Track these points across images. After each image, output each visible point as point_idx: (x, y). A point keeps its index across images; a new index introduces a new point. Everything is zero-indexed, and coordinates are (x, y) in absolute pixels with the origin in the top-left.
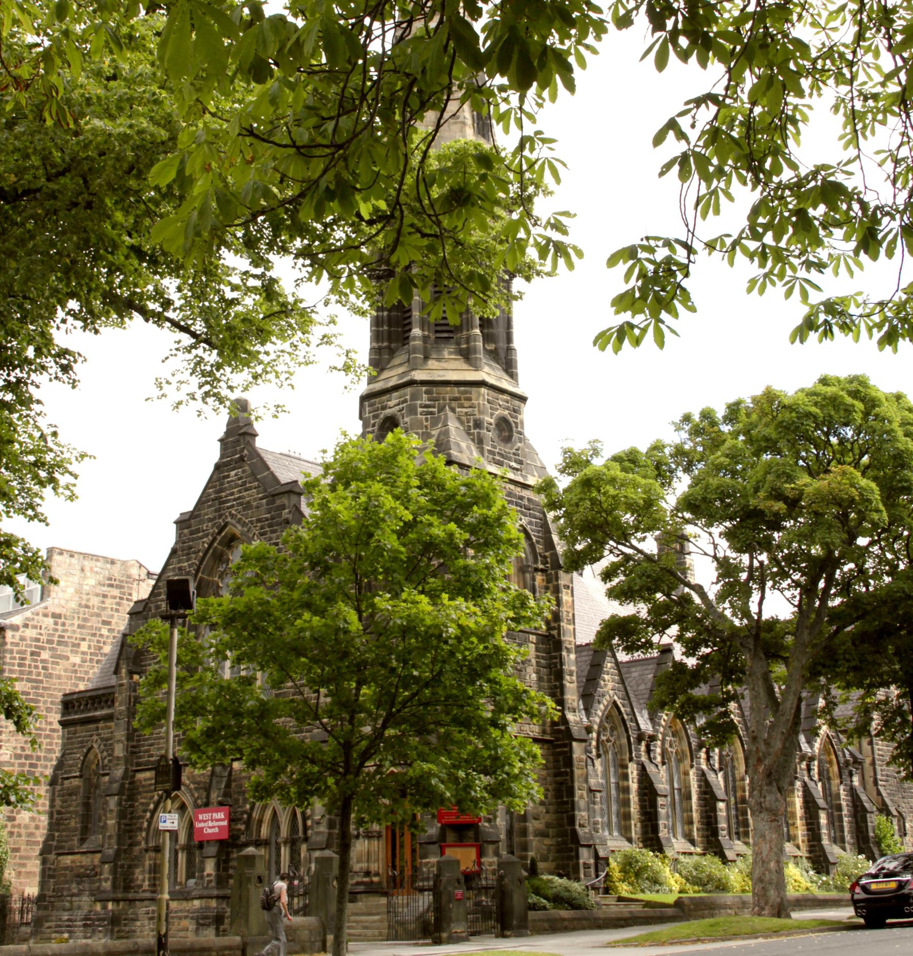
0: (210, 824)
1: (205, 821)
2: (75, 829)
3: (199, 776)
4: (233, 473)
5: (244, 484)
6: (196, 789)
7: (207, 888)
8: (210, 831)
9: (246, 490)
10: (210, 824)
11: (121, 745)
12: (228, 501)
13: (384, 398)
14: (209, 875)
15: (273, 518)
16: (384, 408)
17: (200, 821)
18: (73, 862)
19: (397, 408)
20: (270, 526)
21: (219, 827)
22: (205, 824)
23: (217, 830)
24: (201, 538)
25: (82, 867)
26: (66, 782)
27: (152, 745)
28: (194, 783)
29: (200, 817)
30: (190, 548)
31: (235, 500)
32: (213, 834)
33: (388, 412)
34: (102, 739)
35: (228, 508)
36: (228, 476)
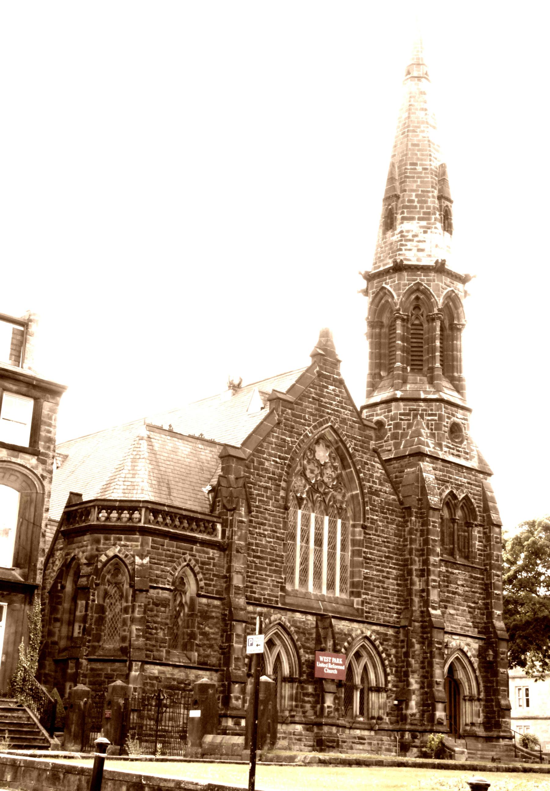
0: (330, 666)
1: (325, 663)
2: (163, 641)
3: (300, 622)
4: (331, 388)
5: (340, 402)
6: (297, 632)
7: (328, 717)
8: (329, 671)
9: (343, 408)
10: (330, 666)
11: (240, 577)
12: (328, 408)
13: (454, 409)
14: (329, 707)
15: (363, 442)
16: (453, 415)
17: (321, 662)
18: (160, 672)
19: (463, 421)
20: (361, 446)
21: (337, 669)
22: (326, 665)
23: (336, 672)
24: (304, 425)
25: (174, 679)
26: (152, 591)
27: (255, 583)
28: (296, 627)
29: (321, 658)
30: (293, 427)
31: (334, 410)
32: (332, 674)
33: (454, 419)
34: (197, 561)
35: (328, 413)
36: (327, 388)
